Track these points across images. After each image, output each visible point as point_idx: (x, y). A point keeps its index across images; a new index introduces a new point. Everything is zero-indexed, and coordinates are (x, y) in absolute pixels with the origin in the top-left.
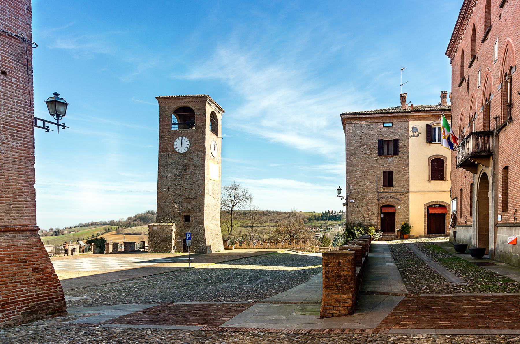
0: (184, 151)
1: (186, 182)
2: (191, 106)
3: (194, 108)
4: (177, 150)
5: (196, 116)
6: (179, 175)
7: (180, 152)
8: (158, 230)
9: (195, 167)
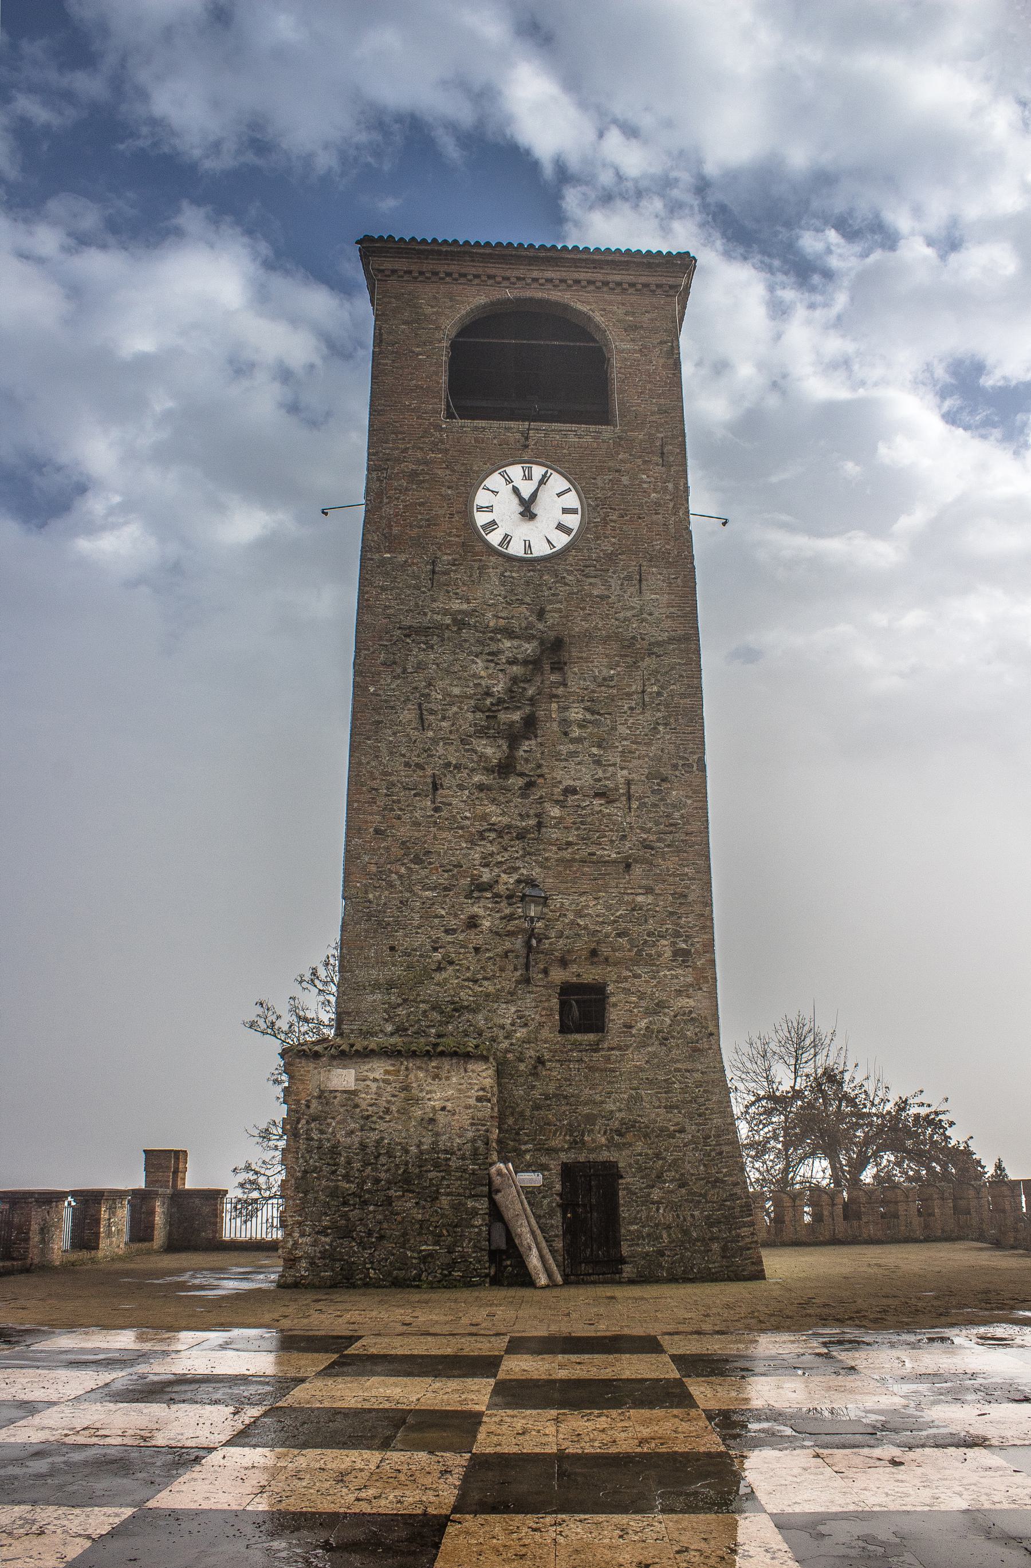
0: (540, 549)
1: (564, 749)
2: (579, 306)
3: (598, 318)
4: (494, 538)
5: (616, 363)
6: (512, 698)
7: (516, 549)
8: (365, 1100)
9: (630, 649)
